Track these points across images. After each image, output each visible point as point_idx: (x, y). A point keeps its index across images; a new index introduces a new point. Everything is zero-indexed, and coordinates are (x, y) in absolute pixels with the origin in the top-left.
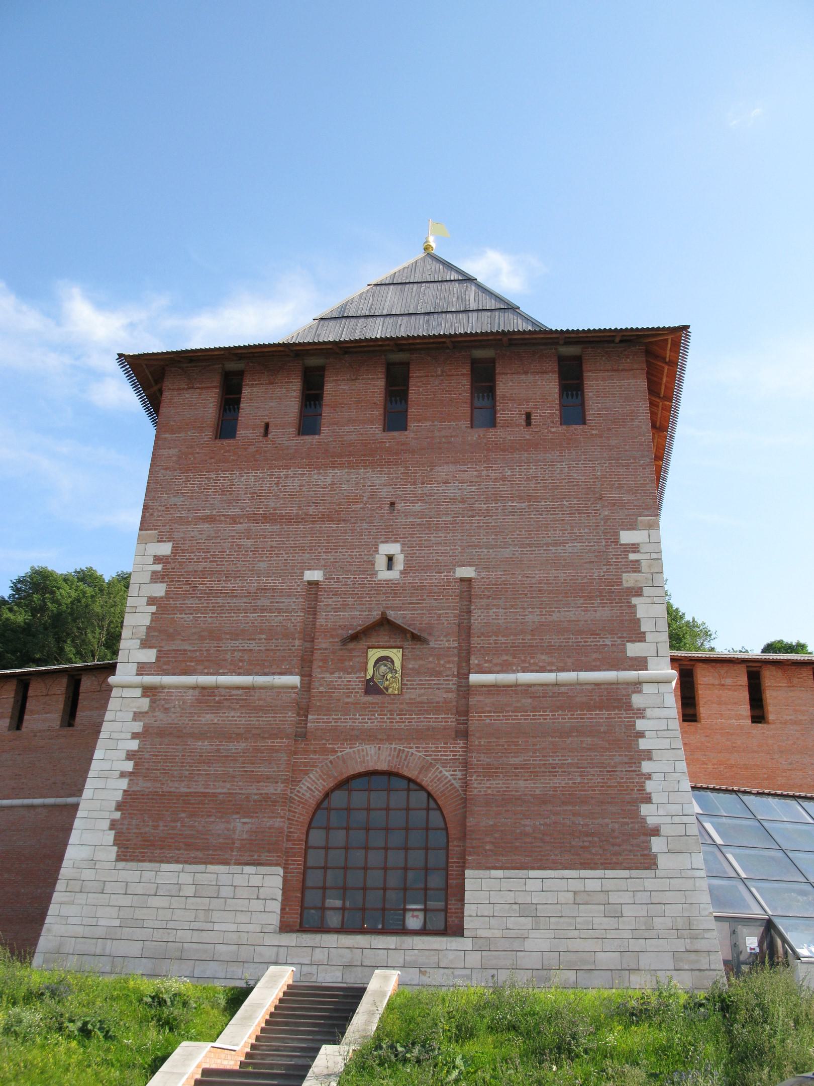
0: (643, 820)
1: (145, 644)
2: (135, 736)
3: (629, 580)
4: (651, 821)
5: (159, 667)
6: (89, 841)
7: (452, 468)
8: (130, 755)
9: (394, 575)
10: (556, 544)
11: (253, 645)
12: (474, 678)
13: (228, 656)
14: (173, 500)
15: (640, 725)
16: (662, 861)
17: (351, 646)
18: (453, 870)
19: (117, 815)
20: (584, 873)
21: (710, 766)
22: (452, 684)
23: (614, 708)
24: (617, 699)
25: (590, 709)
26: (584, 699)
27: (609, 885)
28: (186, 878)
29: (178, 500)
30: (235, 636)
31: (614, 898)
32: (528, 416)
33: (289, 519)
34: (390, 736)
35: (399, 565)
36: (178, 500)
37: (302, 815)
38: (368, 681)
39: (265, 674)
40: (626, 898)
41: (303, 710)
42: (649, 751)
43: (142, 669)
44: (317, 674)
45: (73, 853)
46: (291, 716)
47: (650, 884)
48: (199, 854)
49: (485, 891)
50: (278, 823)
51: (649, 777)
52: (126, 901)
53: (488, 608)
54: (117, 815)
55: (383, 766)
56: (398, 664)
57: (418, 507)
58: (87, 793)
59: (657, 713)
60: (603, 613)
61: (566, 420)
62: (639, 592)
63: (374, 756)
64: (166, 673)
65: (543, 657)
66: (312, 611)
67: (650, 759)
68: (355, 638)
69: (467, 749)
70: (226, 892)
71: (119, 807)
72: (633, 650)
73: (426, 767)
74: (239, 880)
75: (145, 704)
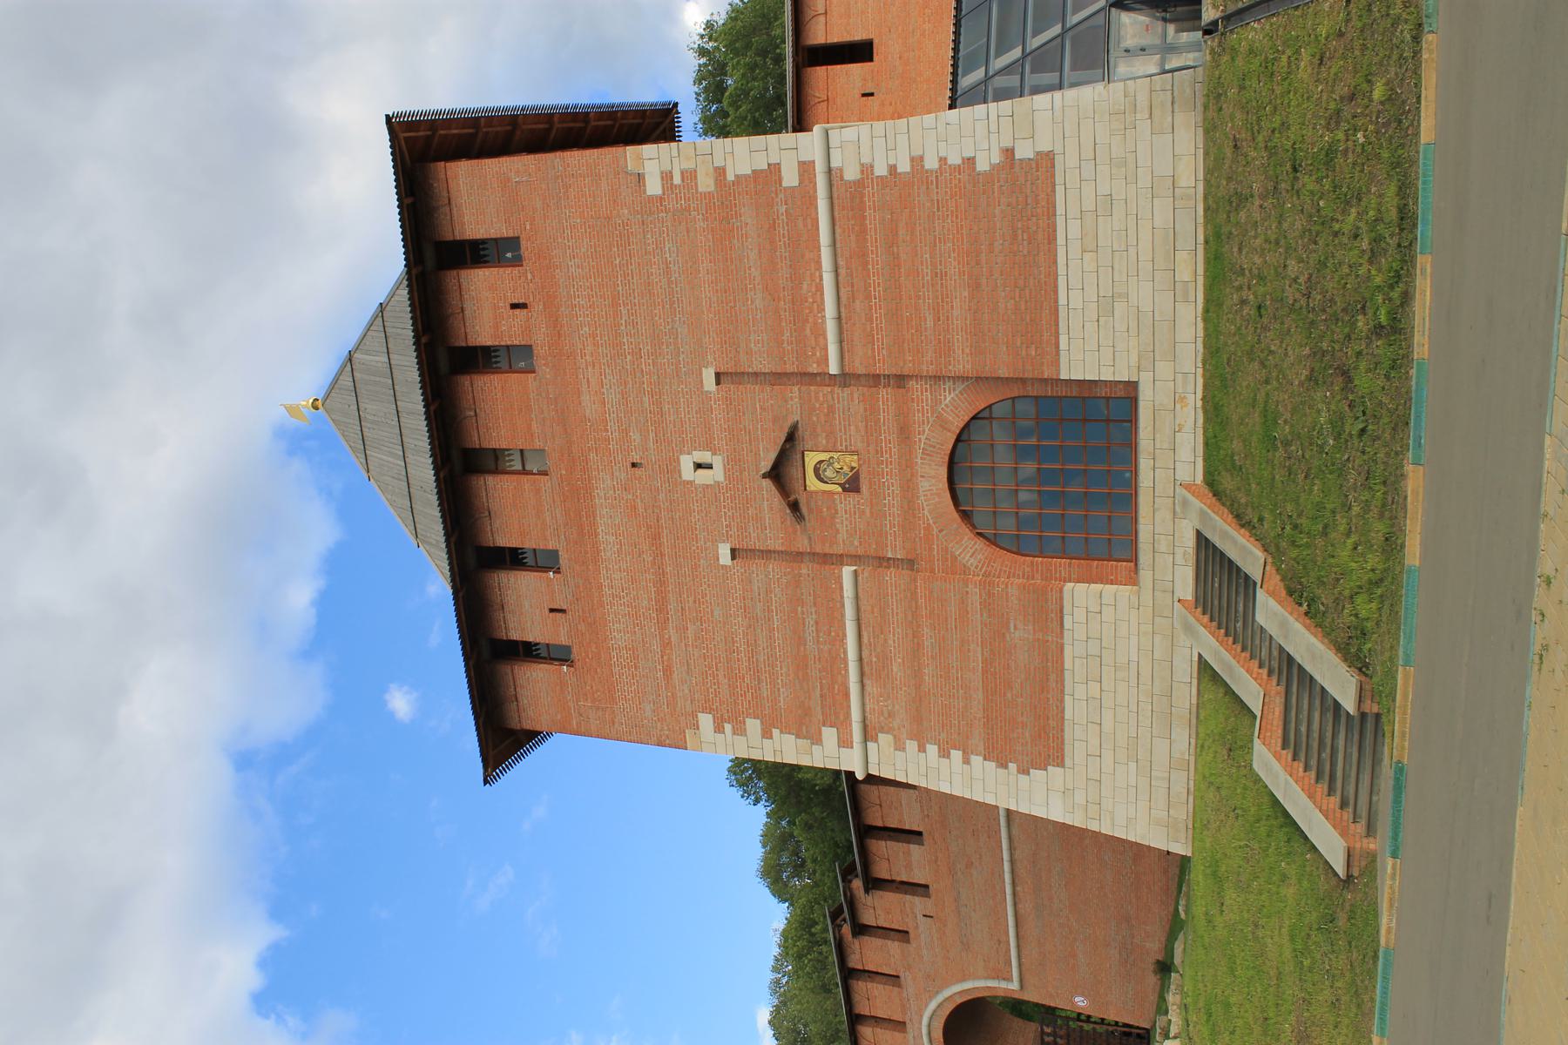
0: (993, 167)
1: (817, 740)
2: (922, 749)
3: (706, 183)
4: (996, 159)
5: (842, 724)
6: (1042, 796)
7: (585, 398)
8: (944, 754)
9: (718, 462)
10: (668, 272)
11: (810, 621)
12: (833, 369)
13: (826, 648)
14: (648, 714)
15: (881, 170)
16: (1045, 146)
17: (804, 510)
18: (1061, 391)
19: (1013, 766)
20: (1060, 240)
21: (927, 26)
22: (842, 394)
23: (862, 202)
24: (851, 198)
25: (863, 231)
26: (853, 237)
27: (1073, 211)
28: (1080, 691)
29: (648, 708)
30: (801, 641)
31: (1089, 205)
32: (514, 306)
33: (661, 583)
34: (907, 465)
35: (705, 457)
36: (648, 708)
37: (1004, 561)
38: (845, 490)
39: (843, 606)
40: (1088, 190)
41: (882, 561)
42: (912, 159)
43: (844, 742)
44: (838, 549)
45: (1057, 812)
46: (890, 575)
47: (1072, 162)
48: (1052, 677)
49: (1084, 357)
50: (1013, 591)
51: (943, 160)
52: (1108, 756)
53: (749, 353)
54: (1013, 766)
55: (943, 472)
56: (824, 456)
57: (635, 436)
58: (990, 800)
59: (865, 149)
60: (748, 216)
61: (517, 261)
62: (720, 172)
63: (932, 480)
64: (848, 715)
65: (805, 286)
67: (922, 158)
68: (794, 507)
69: (919, 377)
70: (1094, 648)
71: (1004, 766)
72: (790, 178)
73: (941, 423)
74: (1080, 634)
75: (885, 739)
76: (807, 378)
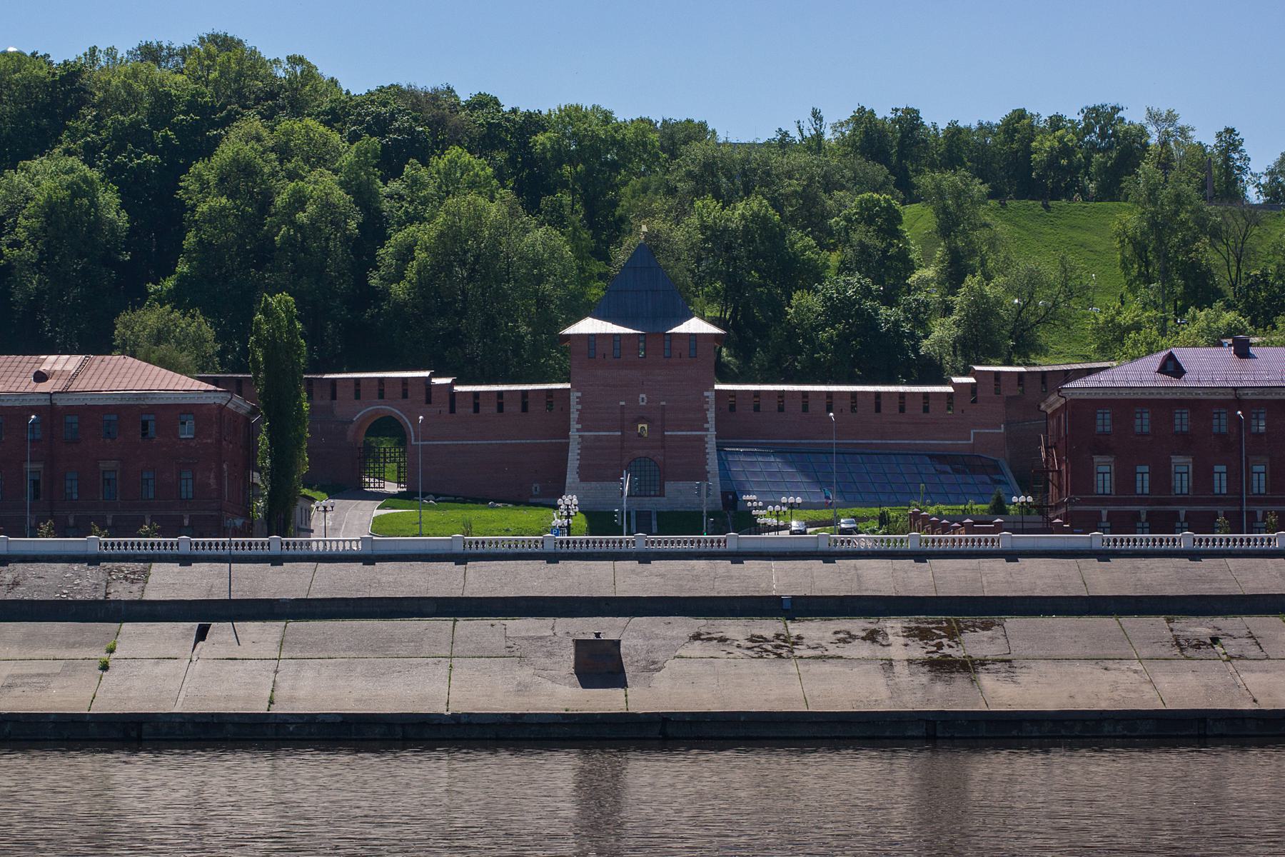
3: (706, 406)
43: (578, 430)
49: (670, 486)
63: (641, 453)
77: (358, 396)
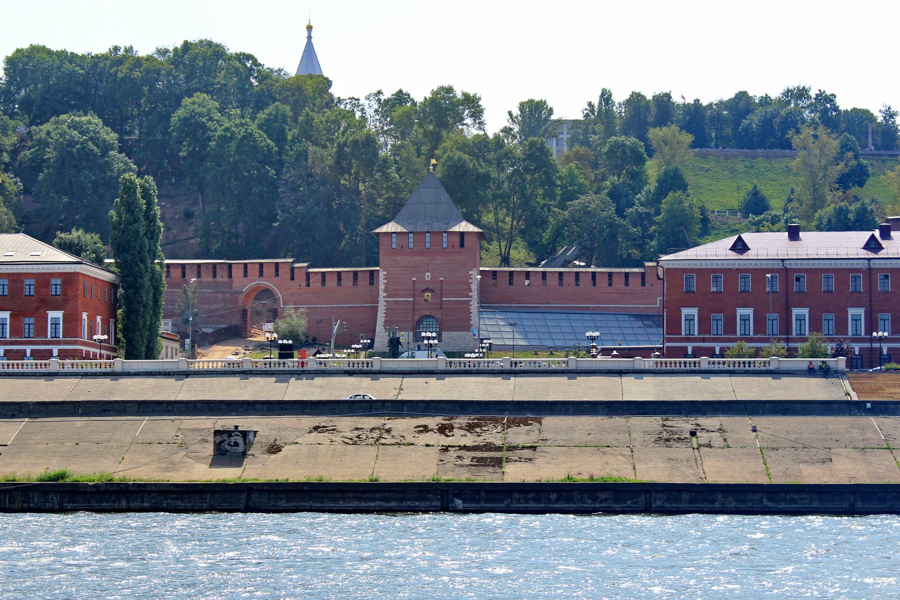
3: (470, 281)
41: (414, 305)
43: (384, 297)
63: (427, 313)
66: (414, 285)
76: (441, 294)
77: (246, 275)
